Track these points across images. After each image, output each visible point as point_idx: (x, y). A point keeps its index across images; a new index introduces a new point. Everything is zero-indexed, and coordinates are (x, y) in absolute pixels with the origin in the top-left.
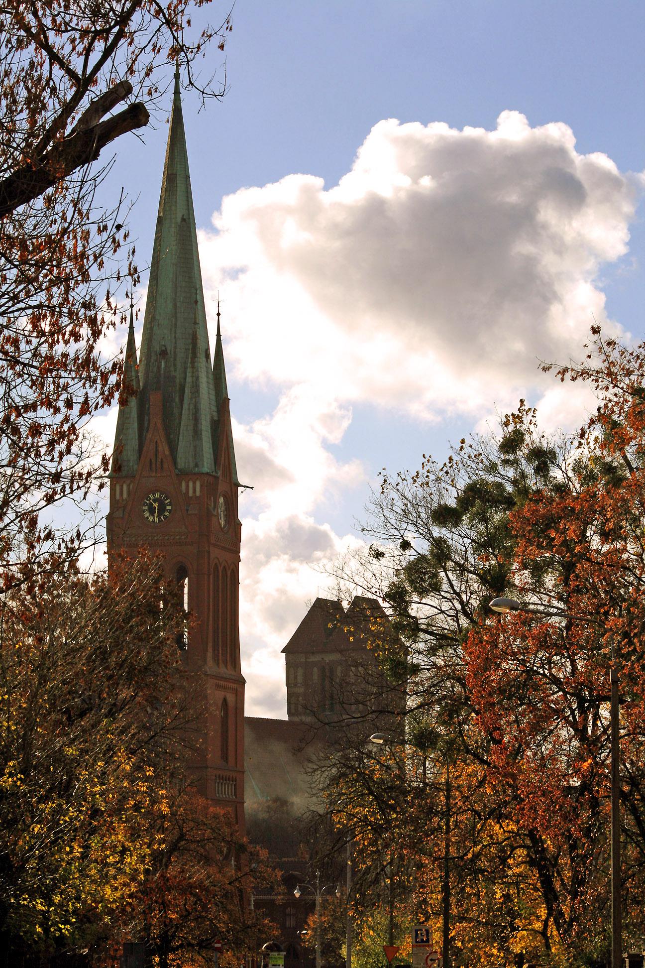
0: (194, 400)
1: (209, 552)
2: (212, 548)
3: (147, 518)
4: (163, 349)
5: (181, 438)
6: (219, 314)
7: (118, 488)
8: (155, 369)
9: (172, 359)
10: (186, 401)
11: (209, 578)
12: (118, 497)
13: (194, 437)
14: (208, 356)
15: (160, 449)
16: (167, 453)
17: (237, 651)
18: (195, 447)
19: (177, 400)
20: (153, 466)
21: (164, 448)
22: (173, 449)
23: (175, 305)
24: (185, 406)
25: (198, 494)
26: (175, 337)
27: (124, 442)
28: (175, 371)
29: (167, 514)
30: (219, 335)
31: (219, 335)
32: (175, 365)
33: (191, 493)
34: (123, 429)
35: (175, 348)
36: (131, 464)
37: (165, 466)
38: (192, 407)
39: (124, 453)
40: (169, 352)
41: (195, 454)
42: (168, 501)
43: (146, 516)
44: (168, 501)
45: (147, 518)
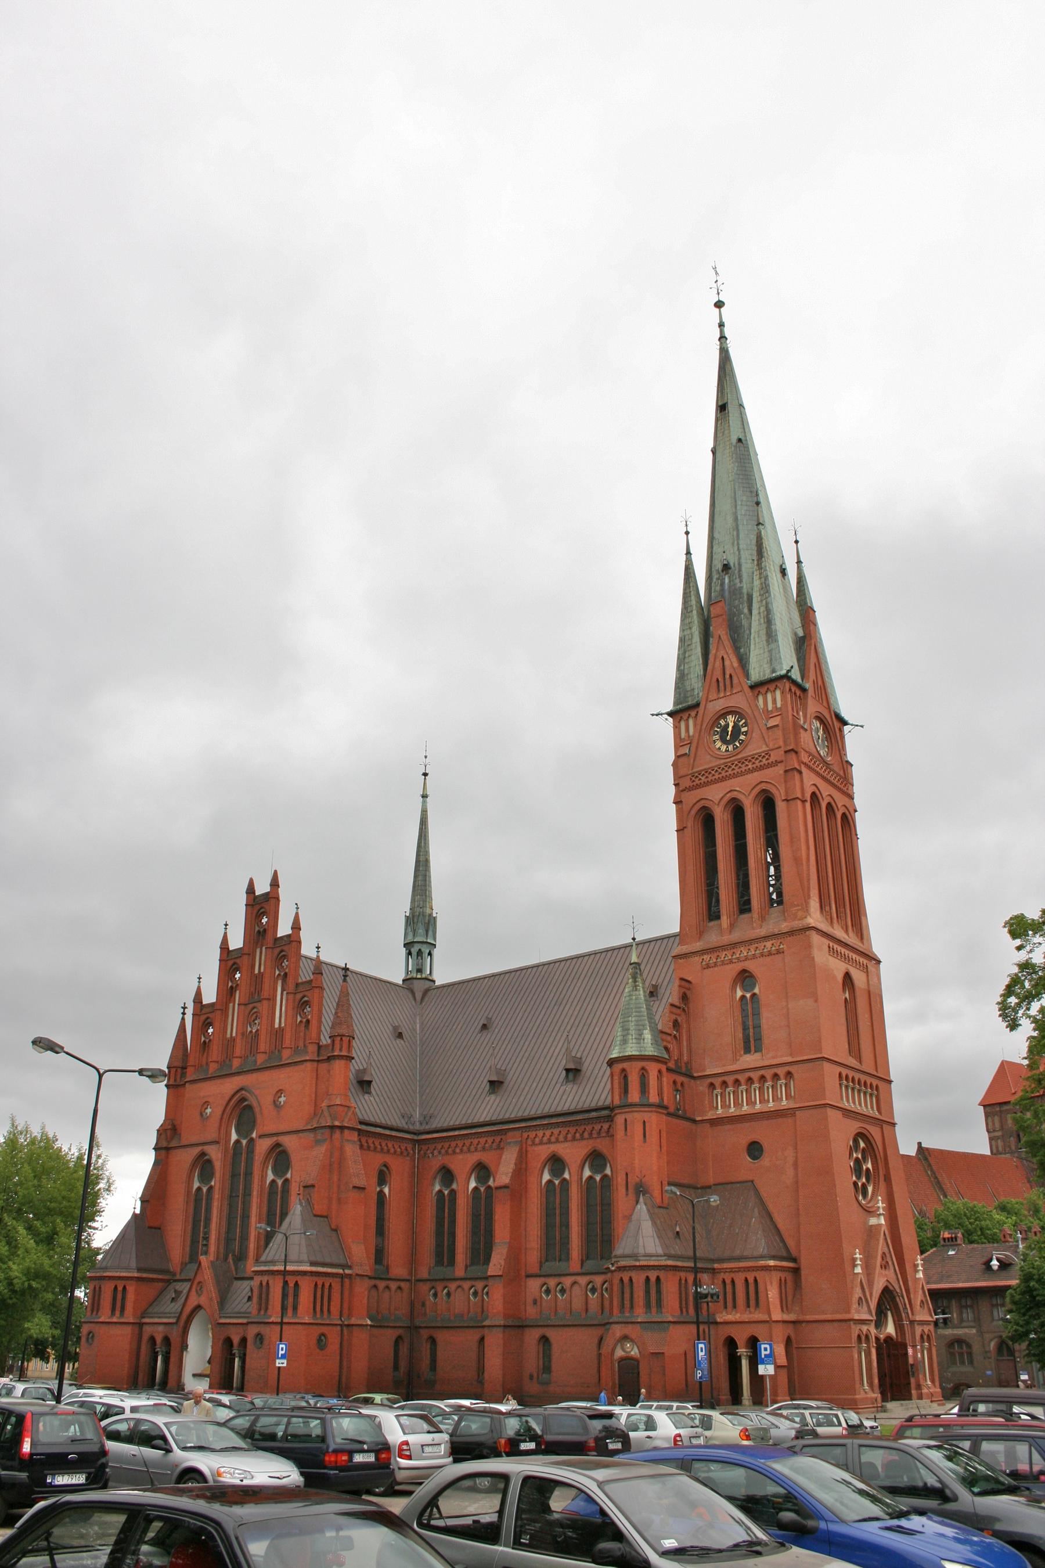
0: (764, 602)
1: (800, 772)
2: (804, 770)
3: (719, 749)
4: (725, 562)
5: (752, 647)
7: (683, 725)
8: (718, 588)
9: (736, 572)
10: (755, 605)
11: (804, 808)
12: (683, 735)
13: (767, 641)
14: (783, 572)
15: (727, 663)
16: (736, 664)
17: (863, 918)
18: (770, 651)
19: (746, 611)
20: (721, 685)
21: (732, 662)
22: (743, 662)
23: (736, 519)
24: (755, 612)
25: (779, 705)
26: (738, 549)
27: (686, 672)
28: (741, 582)
29: (742, 737)
30: (799, 562)
31: (799, 562)
32: (740, 576)
33: (770, 707)
34: (684, 658)
35: (740, 558)
36: (696, 693)
37: (735, 681)
38: (762, 609)
39: (687, 683)
40: (732, 565)
41: (771, 660)
42: (744, 721)
43: (717, 747)
44: (744, 721)
45: (719, 749)
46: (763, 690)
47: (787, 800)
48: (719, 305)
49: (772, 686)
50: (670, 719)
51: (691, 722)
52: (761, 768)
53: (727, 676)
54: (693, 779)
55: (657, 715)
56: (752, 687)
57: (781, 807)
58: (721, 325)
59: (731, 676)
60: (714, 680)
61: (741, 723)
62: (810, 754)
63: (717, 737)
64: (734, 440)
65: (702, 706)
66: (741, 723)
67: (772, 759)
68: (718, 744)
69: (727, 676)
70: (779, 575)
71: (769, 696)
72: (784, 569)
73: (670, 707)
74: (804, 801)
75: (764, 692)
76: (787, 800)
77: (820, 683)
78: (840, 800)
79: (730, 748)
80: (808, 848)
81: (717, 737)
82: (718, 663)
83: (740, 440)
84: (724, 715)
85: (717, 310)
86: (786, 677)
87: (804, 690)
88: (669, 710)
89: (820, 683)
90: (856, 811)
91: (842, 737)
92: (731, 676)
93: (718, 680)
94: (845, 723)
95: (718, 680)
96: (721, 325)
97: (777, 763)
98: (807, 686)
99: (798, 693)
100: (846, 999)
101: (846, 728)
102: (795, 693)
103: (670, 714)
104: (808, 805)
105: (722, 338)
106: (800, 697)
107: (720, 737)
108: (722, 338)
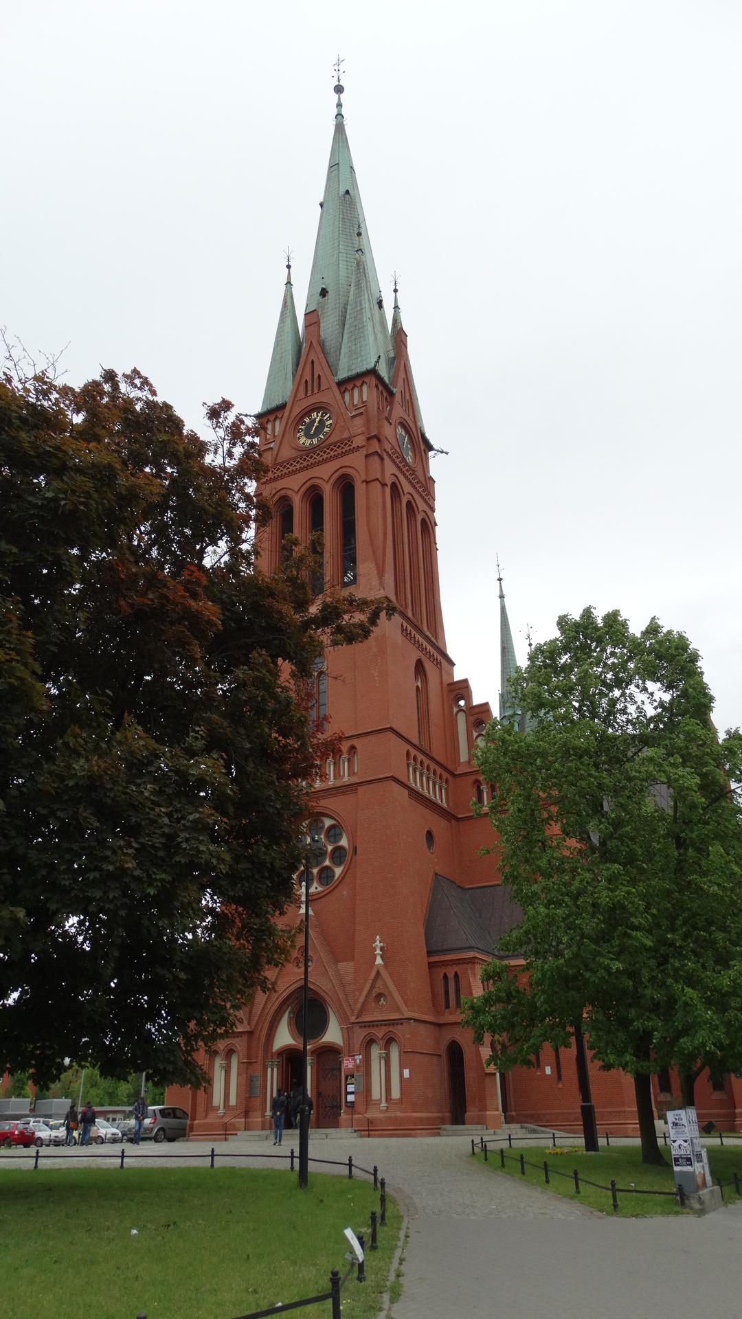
1: (382, 459)
6: (396, 291)
11: (384, 492)
29: (326, 430)
30: (396, 307)
31: (396, 307)
37: (323, 379)
42: (328, 415)
43: (301, 442)
44: (328, 415)
46: (349, 387)
47: (367, 482)
49: (358, 383)
51: (277, 423)
52: (343, 454)
53: (316, 376)
54: (275, 471)
56: (340, 384)
57: (360, 490)
58: (339, 105)
59: (319, 376)
61: (325, 418)
62: (393, 448)
63: (302, 433)
64: (342, 191)
65: (288, 408)
66: (325, 418)
67: (354, 445)
68: (303, 440)
69: (316, 376)
70: (376, 307)
71: (356, 392)
72: (381, 301)
74: (384, 485)
75: (350, 389)
76: (367, 482)
77: (408, 398)
78: (421, 505)
79: (315, 441)
80: (385, 538)
81: (302, 433)
82: (309, 366)
83: (347, 192)
84: (308, 414)
85: (337, 95)
86: (373, 372)
87: (391, 394)
89: (408, 398)
90: (436, 525)
91: (427, 459)
92: (319, 376)
93: (306, 381)
94: (430, 448)
95: (306, 381)
96: (339, 105)
98: (395, 390)
99: (385, 394)
100: (418, 686)
101: (431, 454)
102: (382, 393)
104: (388, 490)
105: (339, 115)
106: (386, 399)
107: (305, 433)
108: (339, 115)
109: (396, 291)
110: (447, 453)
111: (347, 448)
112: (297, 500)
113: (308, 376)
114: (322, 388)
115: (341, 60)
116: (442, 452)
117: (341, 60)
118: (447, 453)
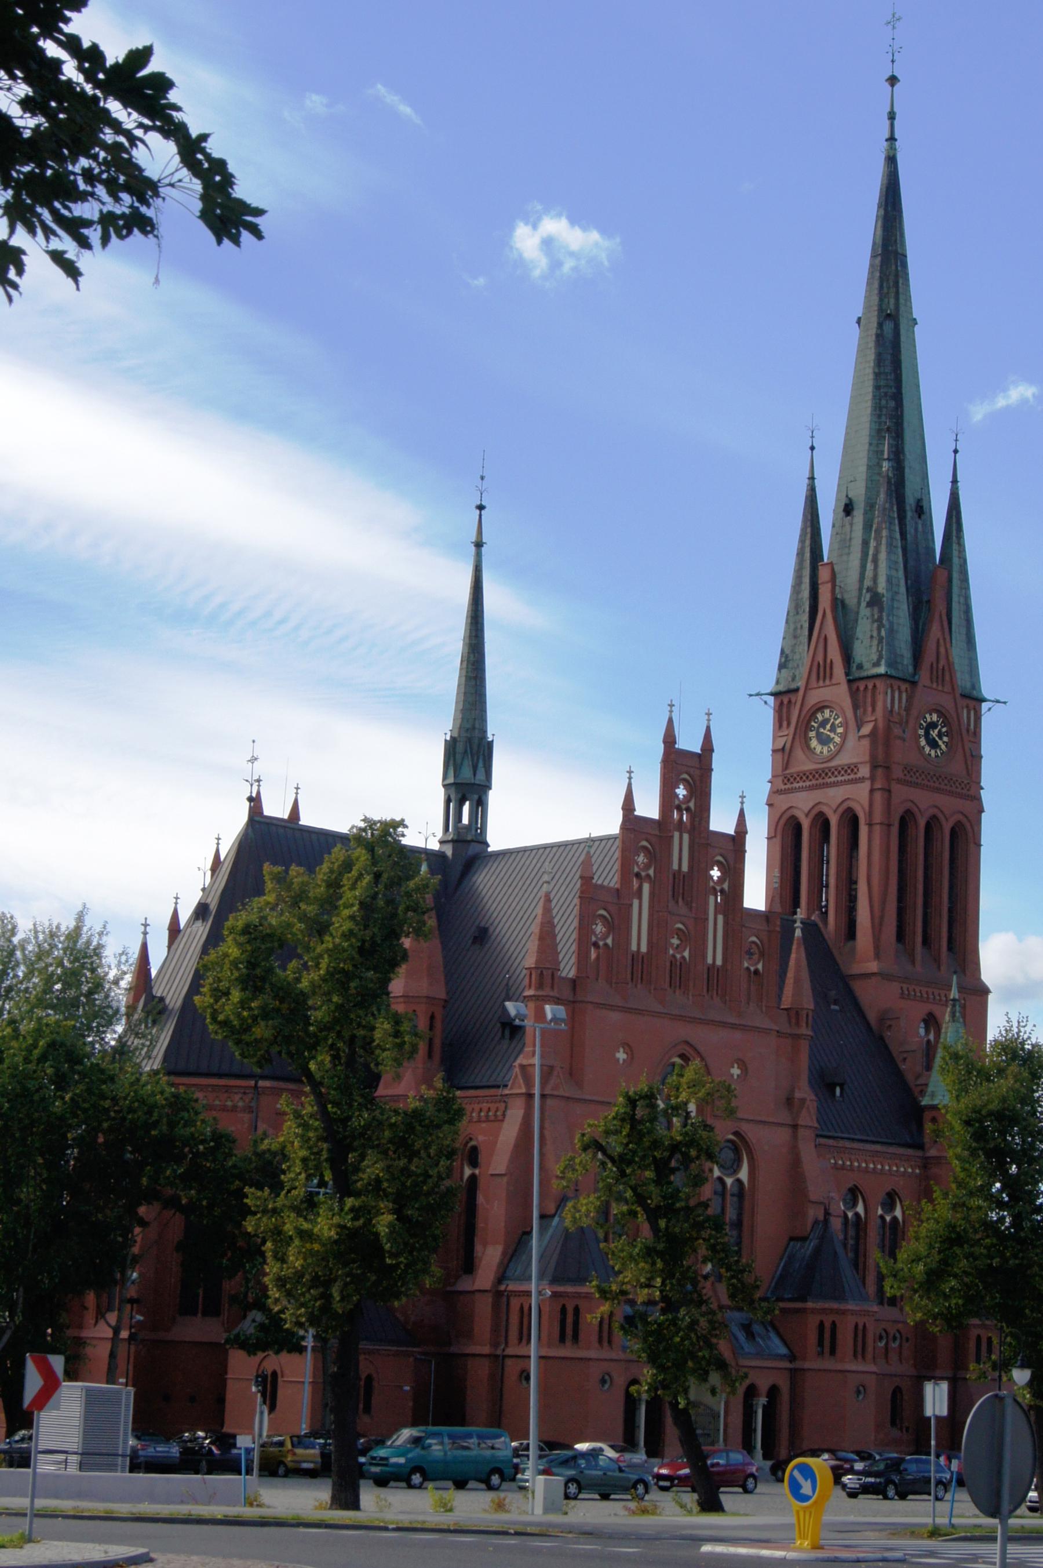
48: (893, 80)
50: (771, 700)
55: (758, 694)
58: (892, 116)
60: (815, 664)
67: (859, 775)
69: (828, 661)
73: (770, 685)
82: (822, 640)
84: (821, 709)
88: (768, 691)
89: (942, 662)
94: (985, 700)
97: (862, 780)
101: (984, 705)
103: (771, 694)
105: (892, 139)
108: (892, 139)
109: (956, 451)
110: (1005, 703)
111: (852, 776)
112: (806, 824)
113: (820, 658)
114: (834, 681)
115: (890, 27)
116: (998, 702)
117: (890, 27)
118: (1005, 703)
